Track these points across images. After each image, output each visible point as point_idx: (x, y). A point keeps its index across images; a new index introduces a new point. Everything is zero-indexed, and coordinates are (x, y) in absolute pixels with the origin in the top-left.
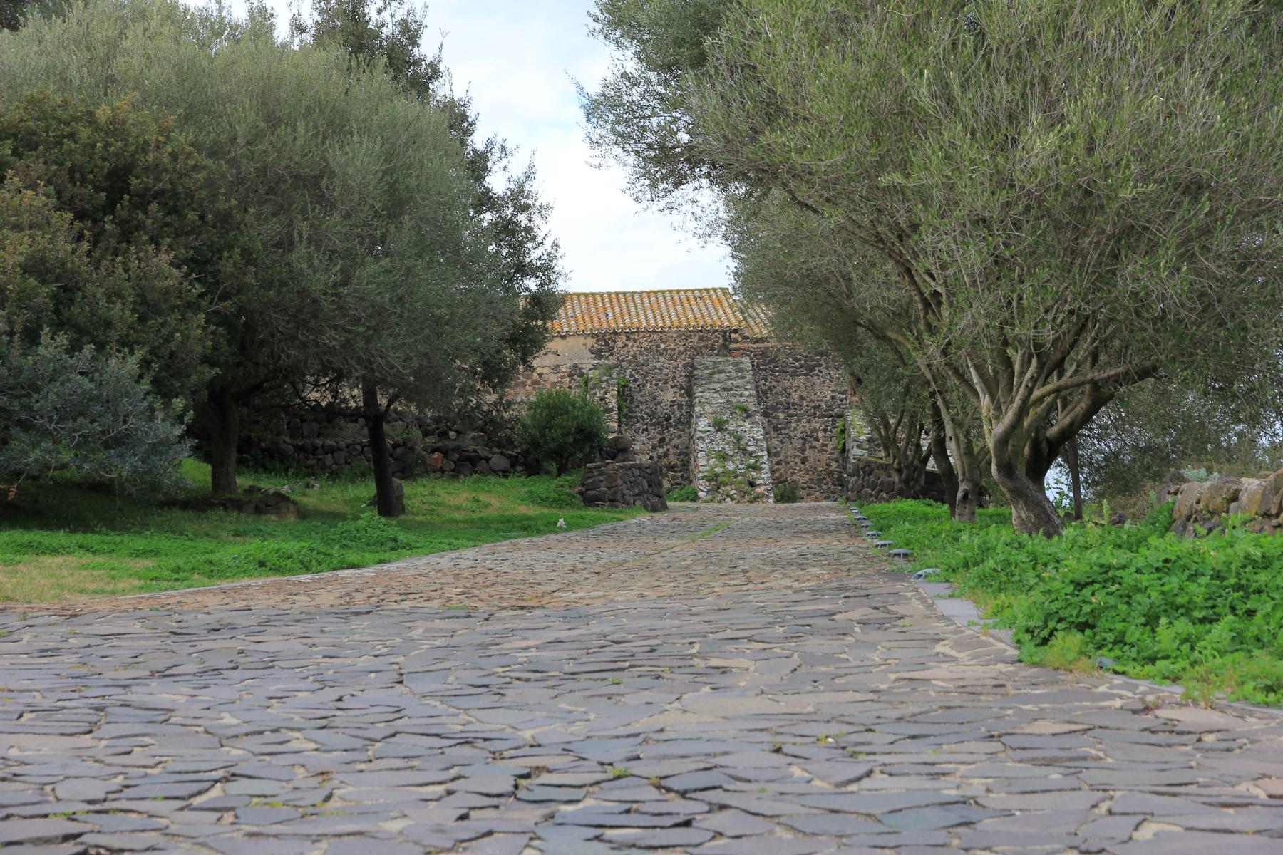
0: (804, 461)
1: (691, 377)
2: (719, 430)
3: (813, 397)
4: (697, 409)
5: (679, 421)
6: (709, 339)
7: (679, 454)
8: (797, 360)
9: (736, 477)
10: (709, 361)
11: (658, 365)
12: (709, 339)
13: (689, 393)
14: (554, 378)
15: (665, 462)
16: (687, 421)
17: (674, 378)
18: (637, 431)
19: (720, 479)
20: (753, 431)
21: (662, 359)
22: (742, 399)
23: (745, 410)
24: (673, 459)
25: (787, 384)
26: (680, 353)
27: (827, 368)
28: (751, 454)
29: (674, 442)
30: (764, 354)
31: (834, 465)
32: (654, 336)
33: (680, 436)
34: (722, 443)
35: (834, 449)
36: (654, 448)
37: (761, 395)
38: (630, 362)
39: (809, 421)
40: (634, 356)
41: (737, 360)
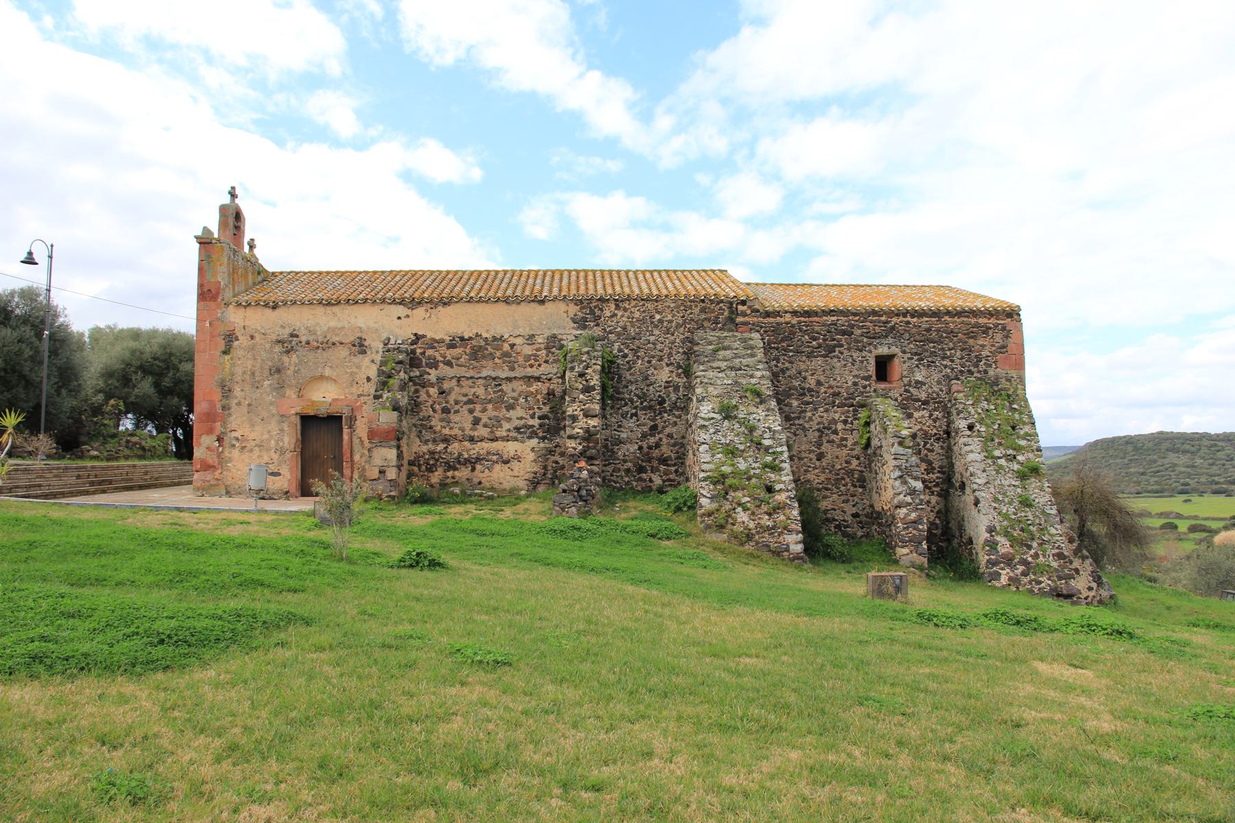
0: (820, 457)
2: (727, 417)
3: (832, 383)
4: (699, 391)
5: (674, 406)
6: (713, 311)
7: (674, 445)
8: (815, 339)
9: (749, 479)
10: (712, 335)
12: (713, 311)
13: (687, 373)
14: (528, 350)
15: (656, 453)
16: (683, 406)
17: (670, 354)
18: (624, 416)
19: (729, 482)
20: (768, 420)
21: (656, 332)
22: (753, 381)
23: (758, 394)
24: (666, 450)
25: (803, 367)
27: (849, 349)
28: (767, 449)
29: (668, 430)
30: (776, 329)
31: (855, 462)
32: (649, 305)
33: (675, 423)
34: (731, 434)
35: (856, 444)
36: (644, 436)
38: (619, 334)
39: (827, 411)
40: (624, 328)
41: (746, 335)
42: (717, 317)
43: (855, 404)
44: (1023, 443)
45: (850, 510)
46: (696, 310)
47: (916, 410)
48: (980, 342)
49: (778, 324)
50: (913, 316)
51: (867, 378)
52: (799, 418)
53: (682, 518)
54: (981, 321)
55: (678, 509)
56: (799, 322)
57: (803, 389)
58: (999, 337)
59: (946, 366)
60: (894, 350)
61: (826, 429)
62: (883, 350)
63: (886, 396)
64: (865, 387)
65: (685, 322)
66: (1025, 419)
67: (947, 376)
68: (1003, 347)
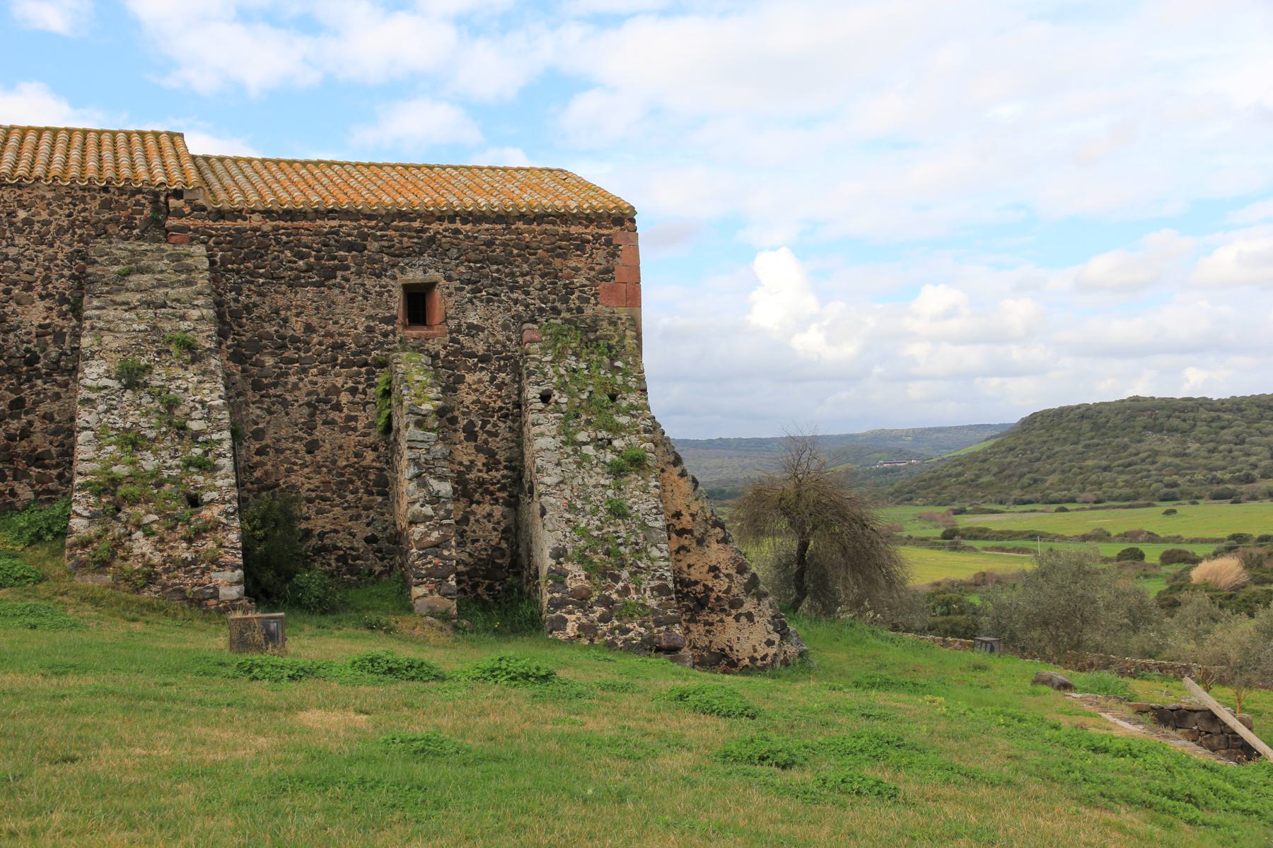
0: (312, 447)
1: (81, 281)
3: (331, 327)
4: (86, 342)
5: (55, 366)
6: (124, 207)
7: (55, 433)
9: (159, 485)
10: (120, 249)
11: (12, 252)
12: (124, 207)
13: (77, 310)
15: (22, 447)
16: (68, 366)
17: (47, 280)
19: (122, 490)
20: (202, 391)
21: (20, 240)
22: (184, 325)
23: (189, 347)
24: (40, 441)
25: (281, 301)
26: (60, 231)
27: (359, 274)
28: (195, 436)
29: (42, 408)
31: (370, 456)
33: (57, 397)
34: (136, 413)
35: (371, 425)
37: (226, 321)
39: (323, 373)
41: (180, 249)
42: (131, 218)
43: (370, 362)
44: (624, 420)
45: (362, 531)
46: (95, 205)
47: (469, 370)
48: (572, 264)
49: (238, 231)
50: (465, 221)
51: (390, 320)
52: (275, 385)
53: (42, 552)
54: (574, 229)
55: (37, 538)
56: (276, 229)
57: (283, 338)
58: (600, 255)
59: (516, 302)
60: (434, 275)
61: (321, 403)
62: (415, 276)
63: (418, 349)
64: (385, 335)
65: (72, 224)
66: (632, 383)
67: (518, 317)
68: (608, 271)
